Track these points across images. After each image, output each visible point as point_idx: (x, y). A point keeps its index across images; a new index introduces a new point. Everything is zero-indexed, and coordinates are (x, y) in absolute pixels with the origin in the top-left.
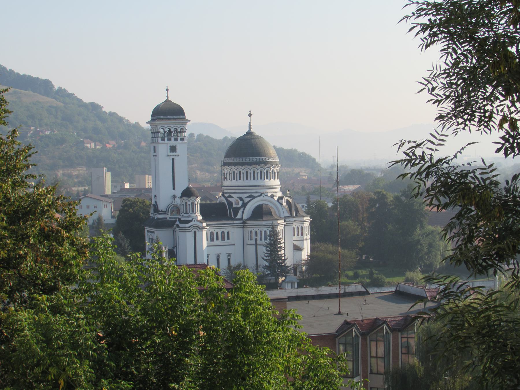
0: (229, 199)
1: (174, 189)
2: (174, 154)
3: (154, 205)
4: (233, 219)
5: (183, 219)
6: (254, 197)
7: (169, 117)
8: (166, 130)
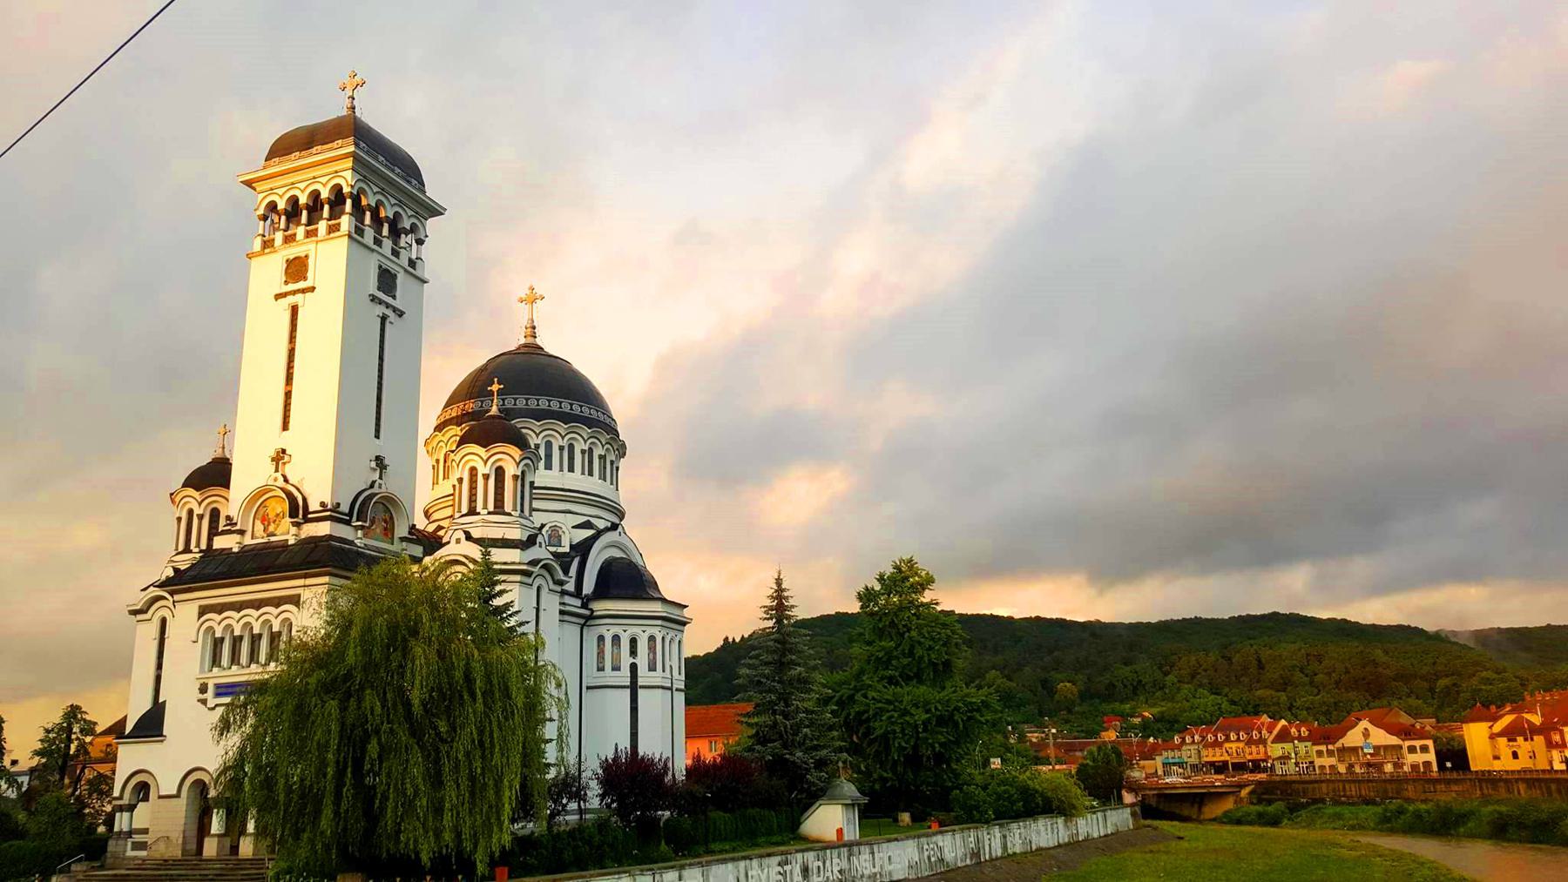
6: (599, 533)
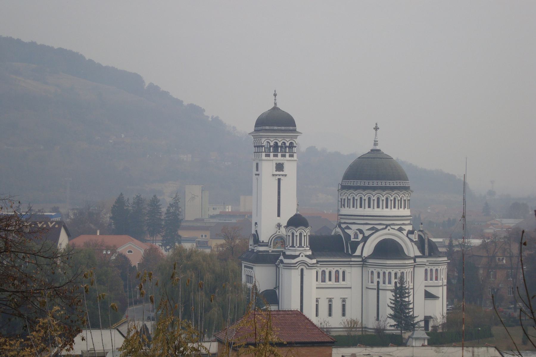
0: (346, 231)
1: (279, 215)
2: (281, 173)
3: (254, 235)
4: (351, 256)
5: (288, 253)
6: (377, 230)
7: (276, 128)
8: (272, 144)
